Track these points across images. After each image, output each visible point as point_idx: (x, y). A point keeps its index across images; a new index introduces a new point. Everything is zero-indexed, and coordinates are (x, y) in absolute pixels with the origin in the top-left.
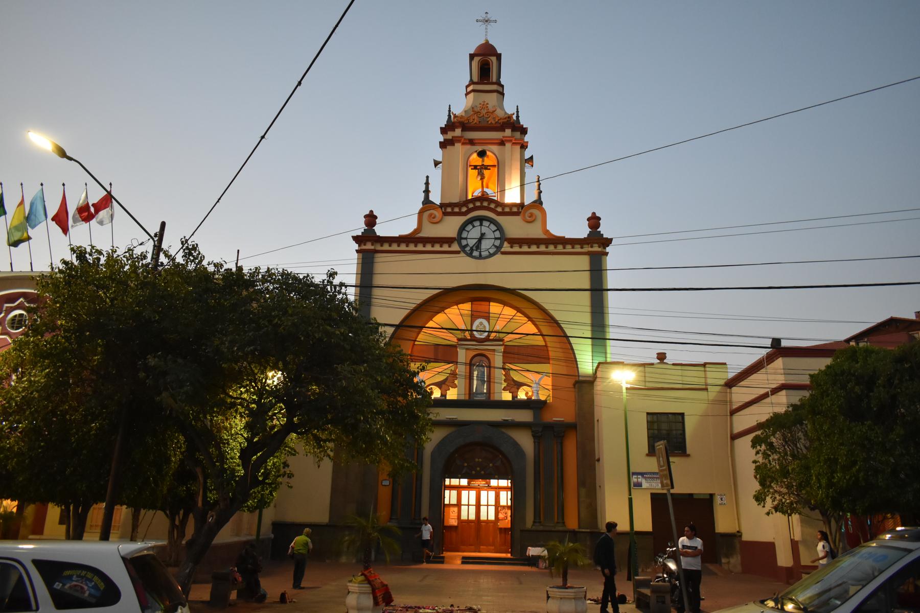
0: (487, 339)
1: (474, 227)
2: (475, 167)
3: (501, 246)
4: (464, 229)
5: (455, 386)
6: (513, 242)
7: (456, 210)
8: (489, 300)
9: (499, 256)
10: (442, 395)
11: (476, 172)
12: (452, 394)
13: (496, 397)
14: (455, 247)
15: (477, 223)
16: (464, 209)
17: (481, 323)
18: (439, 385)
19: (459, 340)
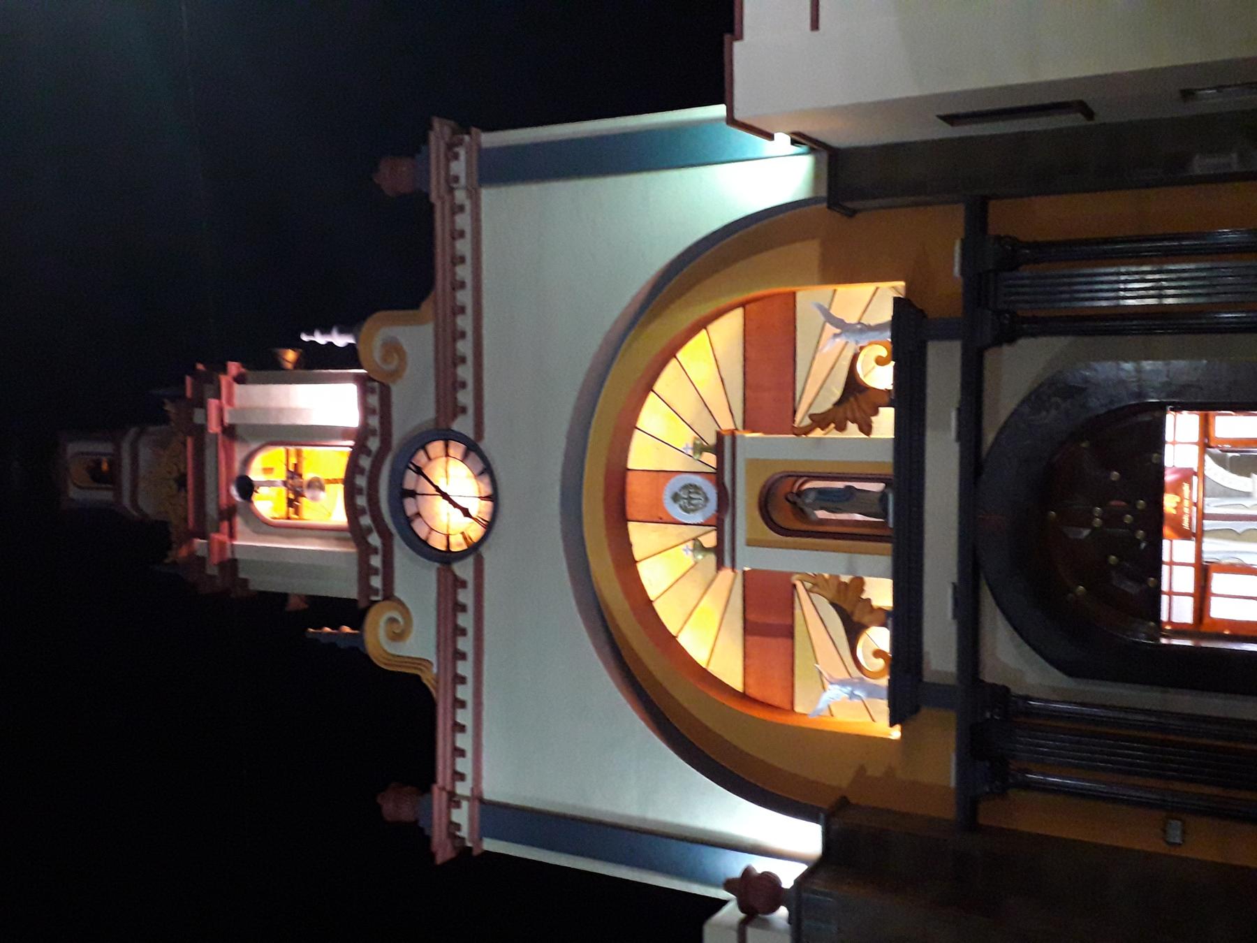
0: (717, 477)
1: (418, 515)
2: (290, 503)
3: (460, 438)
4: (425, 543)
5: (859, 584)
6: (448, 407)
7: (376, 561)
8: (618, 476)
9: (484, 445)
10: (884, 625)
11: (305, 502)
12: (881, 593)
13: (887, 457)
14: (464, 570)
15: (410, 506)
16: (375, 540)
17: (676, 498)
18: (854, 631)
19: (720, 565)
